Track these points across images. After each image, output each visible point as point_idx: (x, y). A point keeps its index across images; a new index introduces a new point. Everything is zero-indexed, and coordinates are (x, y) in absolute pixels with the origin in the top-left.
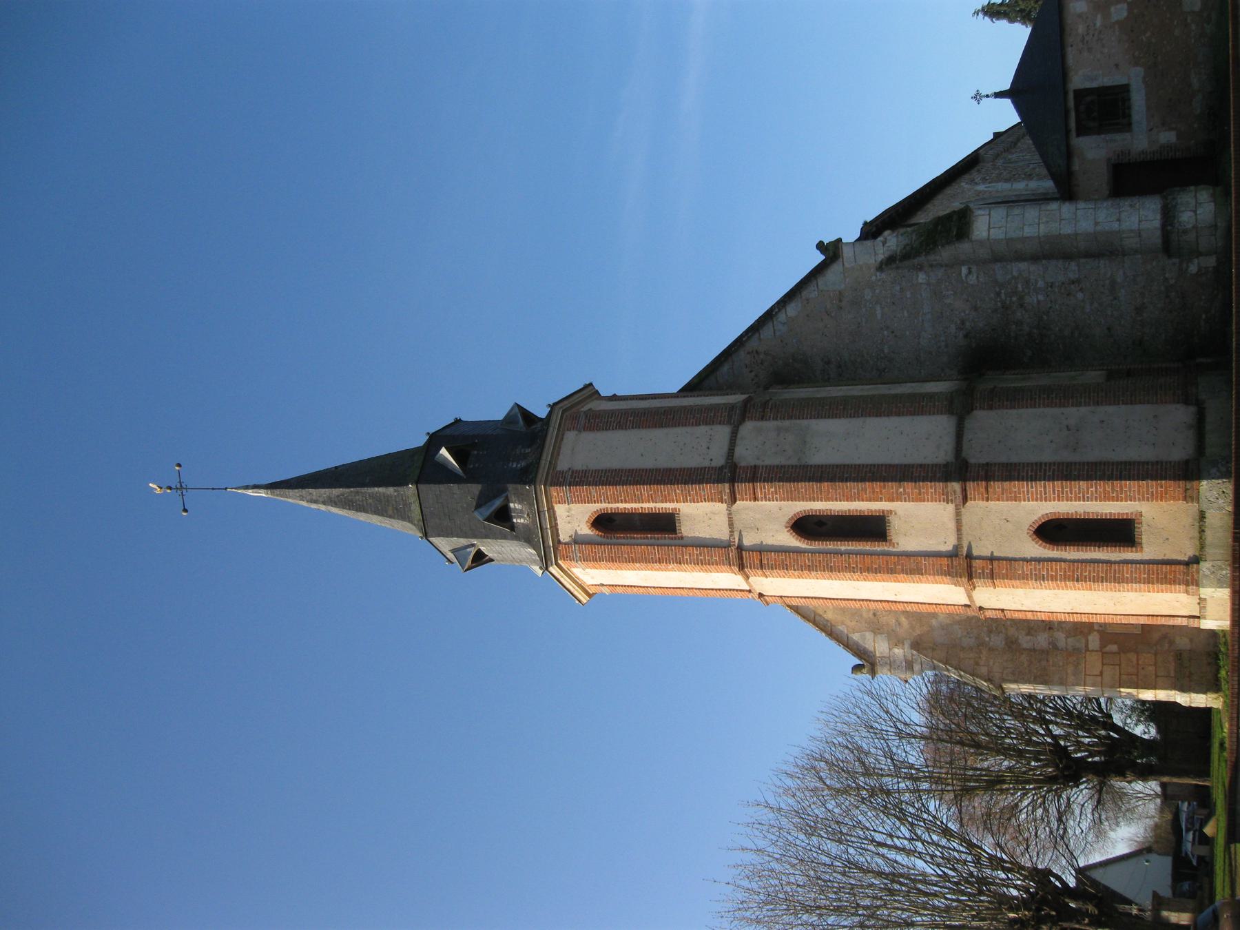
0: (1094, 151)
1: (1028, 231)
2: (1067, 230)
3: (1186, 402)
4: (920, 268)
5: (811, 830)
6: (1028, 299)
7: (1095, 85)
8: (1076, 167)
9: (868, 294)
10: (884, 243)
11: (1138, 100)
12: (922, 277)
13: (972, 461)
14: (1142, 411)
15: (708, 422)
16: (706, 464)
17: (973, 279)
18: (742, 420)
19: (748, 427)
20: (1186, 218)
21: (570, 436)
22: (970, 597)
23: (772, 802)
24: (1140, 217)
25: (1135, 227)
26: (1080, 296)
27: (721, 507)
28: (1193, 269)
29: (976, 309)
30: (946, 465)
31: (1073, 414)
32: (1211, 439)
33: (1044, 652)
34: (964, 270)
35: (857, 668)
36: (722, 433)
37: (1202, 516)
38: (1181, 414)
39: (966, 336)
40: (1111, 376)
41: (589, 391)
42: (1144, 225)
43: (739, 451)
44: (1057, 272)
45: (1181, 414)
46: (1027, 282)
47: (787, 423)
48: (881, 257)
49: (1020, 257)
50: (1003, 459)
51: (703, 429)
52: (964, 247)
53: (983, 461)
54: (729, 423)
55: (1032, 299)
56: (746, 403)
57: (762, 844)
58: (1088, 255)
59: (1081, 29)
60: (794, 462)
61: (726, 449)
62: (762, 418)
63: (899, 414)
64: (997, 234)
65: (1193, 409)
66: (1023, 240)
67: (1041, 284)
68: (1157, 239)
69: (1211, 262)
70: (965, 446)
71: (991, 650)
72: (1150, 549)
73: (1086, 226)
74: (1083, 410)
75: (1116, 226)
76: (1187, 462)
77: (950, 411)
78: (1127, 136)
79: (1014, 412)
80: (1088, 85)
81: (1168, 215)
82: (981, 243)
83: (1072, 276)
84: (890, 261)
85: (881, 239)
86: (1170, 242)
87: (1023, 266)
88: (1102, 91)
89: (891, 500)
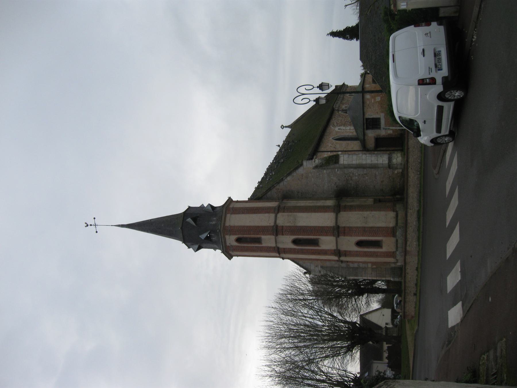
0: (371, 134)
1: (354, 162)
2: (364, 162)
3: (394, 211)
4: (325, 169)
5: (286, 314)
6: (353, 178)
7: (371, 117)
8: (366, 138)
9: (310, 175)
10: (315, 161)
11: (383, 122)
12: (325, 171)
13: (340, 226)
14: (383, 213)
15: (268, 212)
16: (268, 225)
17: (338, 172)
18: (278, 213)
19: (279, 215)
20: (394, 161)
21: (228, 216)
22: (339, 258)
23: (274, 307)
24: (382, 159)
25: (381, 162)
26: (367, 178)
27: (273, 237)
28: (396, 172)
29: (339, 180)
30: (334, 227)
31: (366, 213)
32: (399, 221)
33: (357, 268)
34: (336, 170)
35: (305, 273)
36: (273, 216)
37: (397, 241)
38: (392, 214)
39: (337, 187)
40: (375, 201)
41: (230, 200)
42: (384, 162)
43: (278, 222)
44: (361, 172)
45: (392, 214)
46: (353, 174)
47: (290, 214)
48: (314, 166)
49: (351, 168)
50: (348, 226)
51: (267, 215)
52: (337, 165)
53: (343, 226)
54: (274, 213)
55: (354, 178)
56: (279, 207)
57: (272, 319)
58: (369, 168)
59: (368, 102)
60: (293, 225)
61: (273, 221)
62: (284, 212)
63: (321, 212)
64: (346, 163)
65: (395, 213)
66: (353, 164)
67: (357, 174)
68: (387, 166)
69: (401, 171)
70: (338, 221)
71: (342, 267)
72: (384, 249)
73: (369, 162)
74: (368, 212)
75: (376, 162)
76: (393, 227)
77: (334, 212)
78: (379, 131)
79: (350, 212)
80: (370, 117)
81: (390, 159)
82: (341, 165)
83: (365, 173)
84: (316, 167)
85: (313, 160)
86: (390, 166)
87: (352, 169)
88: (373, 119)
89: (319, 236)
